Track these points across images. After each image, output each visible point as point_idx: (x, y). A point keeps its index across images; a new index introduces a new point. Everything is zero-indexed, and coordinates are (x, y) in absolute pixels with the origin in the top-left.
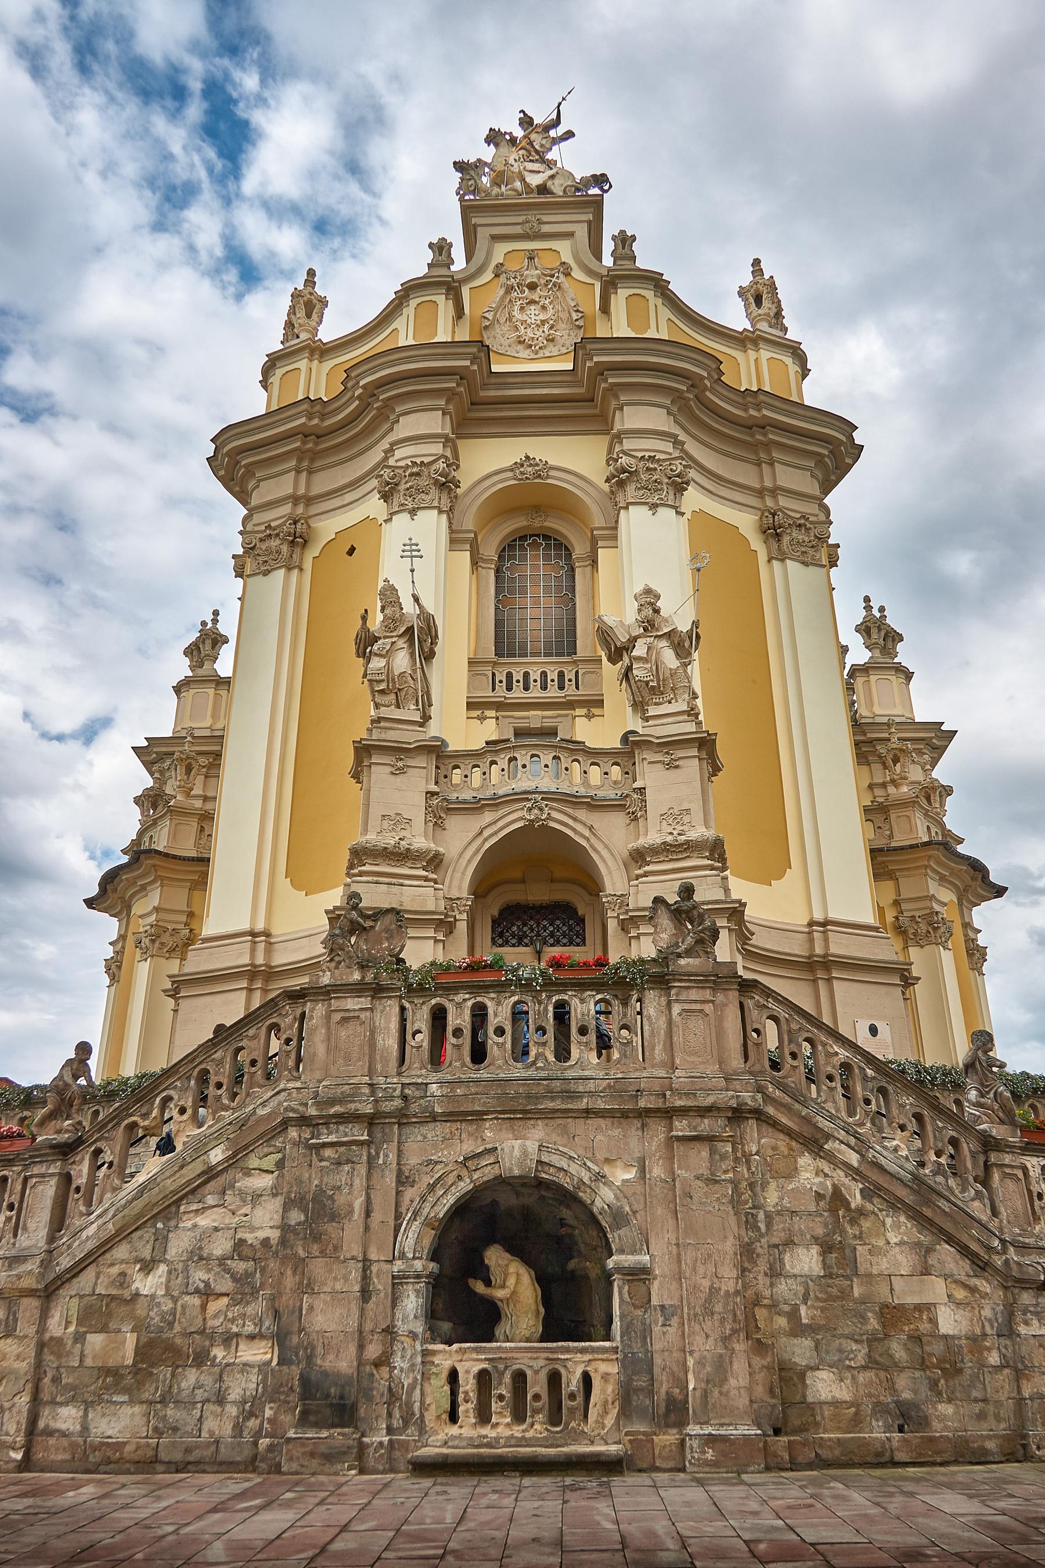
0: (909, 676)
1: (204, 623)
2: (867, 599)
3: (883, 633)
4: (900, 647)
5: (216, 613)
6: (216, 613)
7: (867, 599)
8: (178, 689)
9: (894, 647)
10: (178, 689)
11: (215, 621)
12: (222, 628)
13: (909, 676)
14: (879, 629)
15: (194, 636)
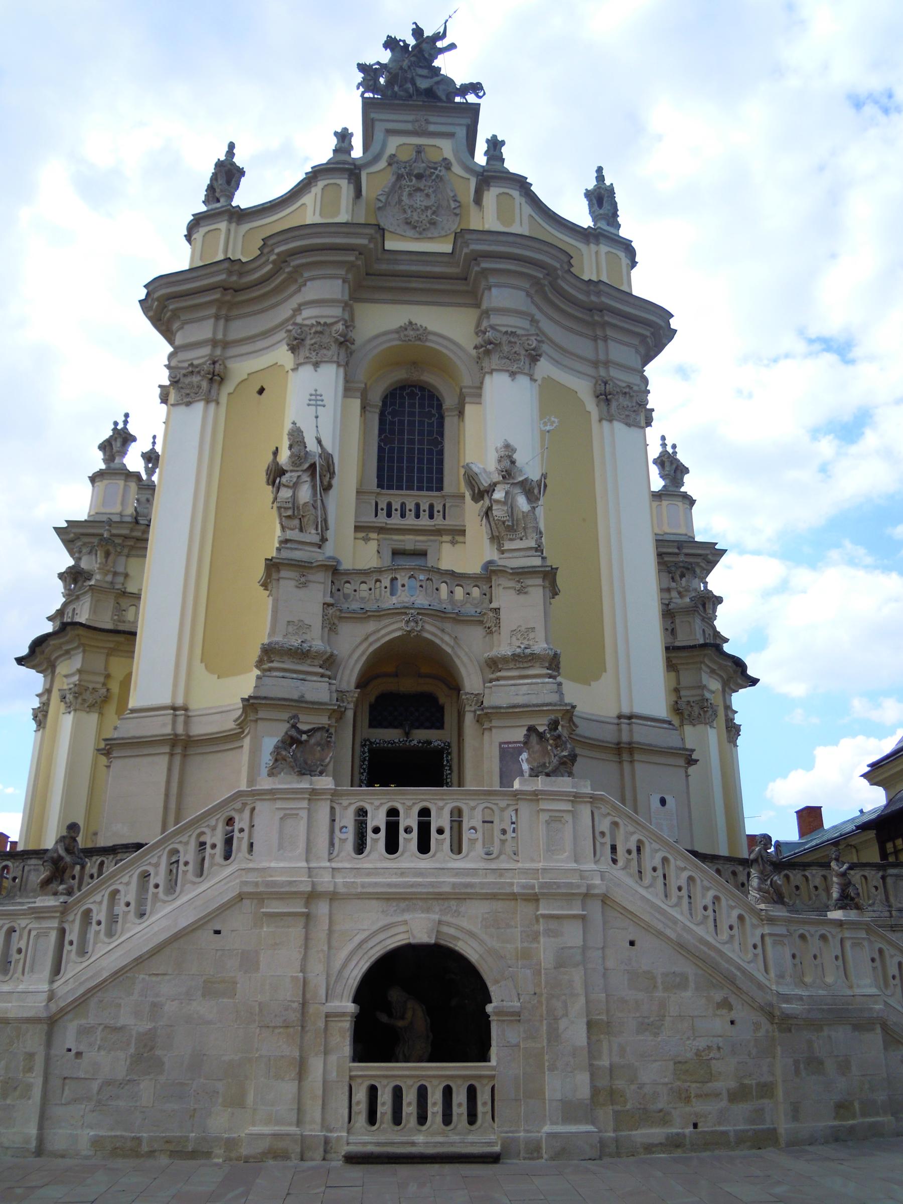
1: (116, 424)
5: (127, 415)
6: (127, 415)
8: (94, 479)
10: (93, 479)
11: (126, 422)
12: (132, 429)
15: (107, 433)
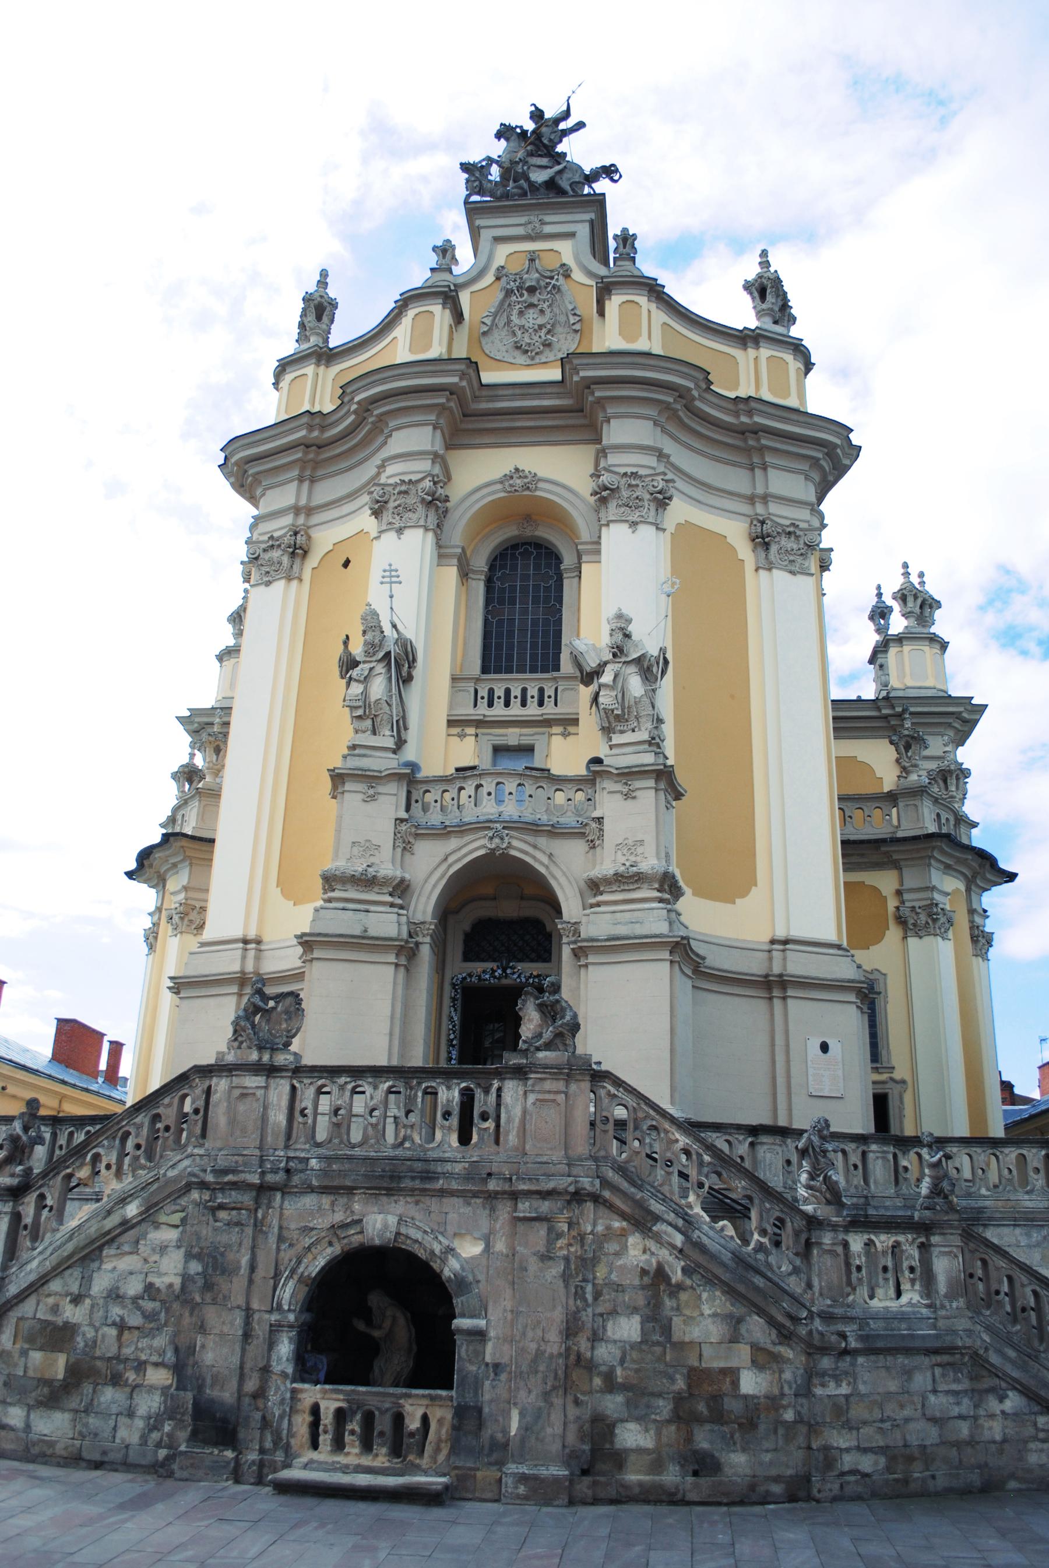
0: (944, 646)
2: (905, 566)
3: (919, 601)
4: (938, 614)
7: (905, 566)
9: (932, 615)
13: (944, 646)
14: (916, 597)
